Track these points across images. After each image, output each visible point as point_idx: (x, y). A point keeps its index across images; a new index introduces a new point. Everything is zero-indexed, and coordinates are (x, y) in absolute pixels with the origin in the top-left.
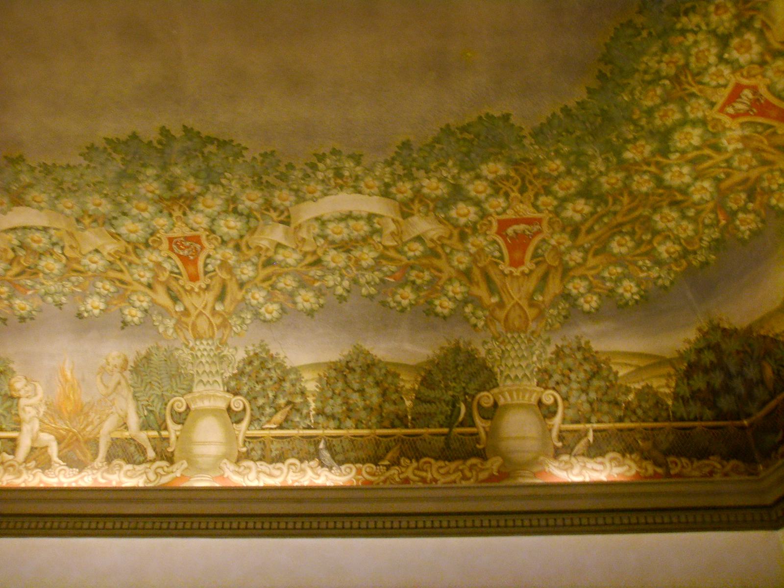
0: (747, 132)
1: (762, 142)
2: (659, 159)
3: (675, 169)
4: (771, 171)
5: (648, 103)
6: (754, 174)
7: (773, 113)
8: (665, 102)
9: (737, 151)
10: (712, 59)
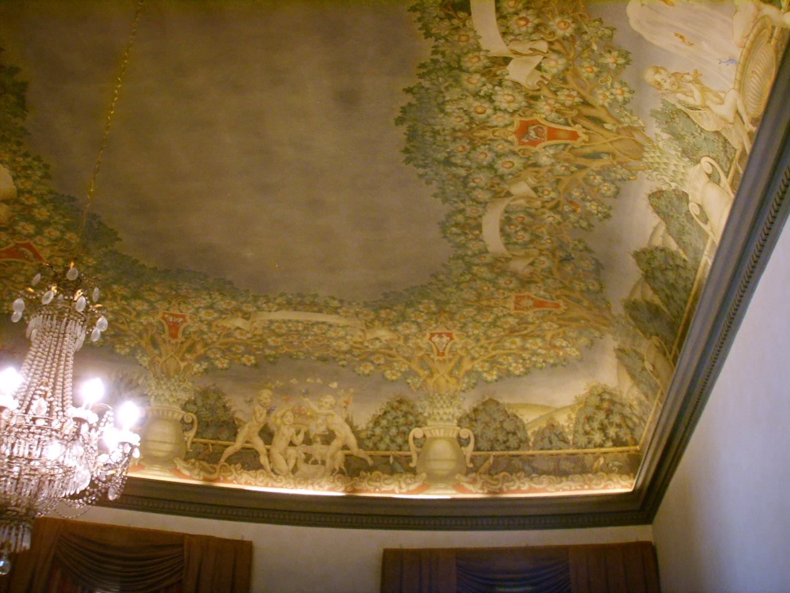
0: (155, 324)
1: (152, 330)
2: (119, 297)
3: (115, 304)
4: (136, 339)
5: (156, 289)
6: (130, 333)
7: (173, 331)
8: (160, 294)
9: (141, 323)
10: (196, 306)
